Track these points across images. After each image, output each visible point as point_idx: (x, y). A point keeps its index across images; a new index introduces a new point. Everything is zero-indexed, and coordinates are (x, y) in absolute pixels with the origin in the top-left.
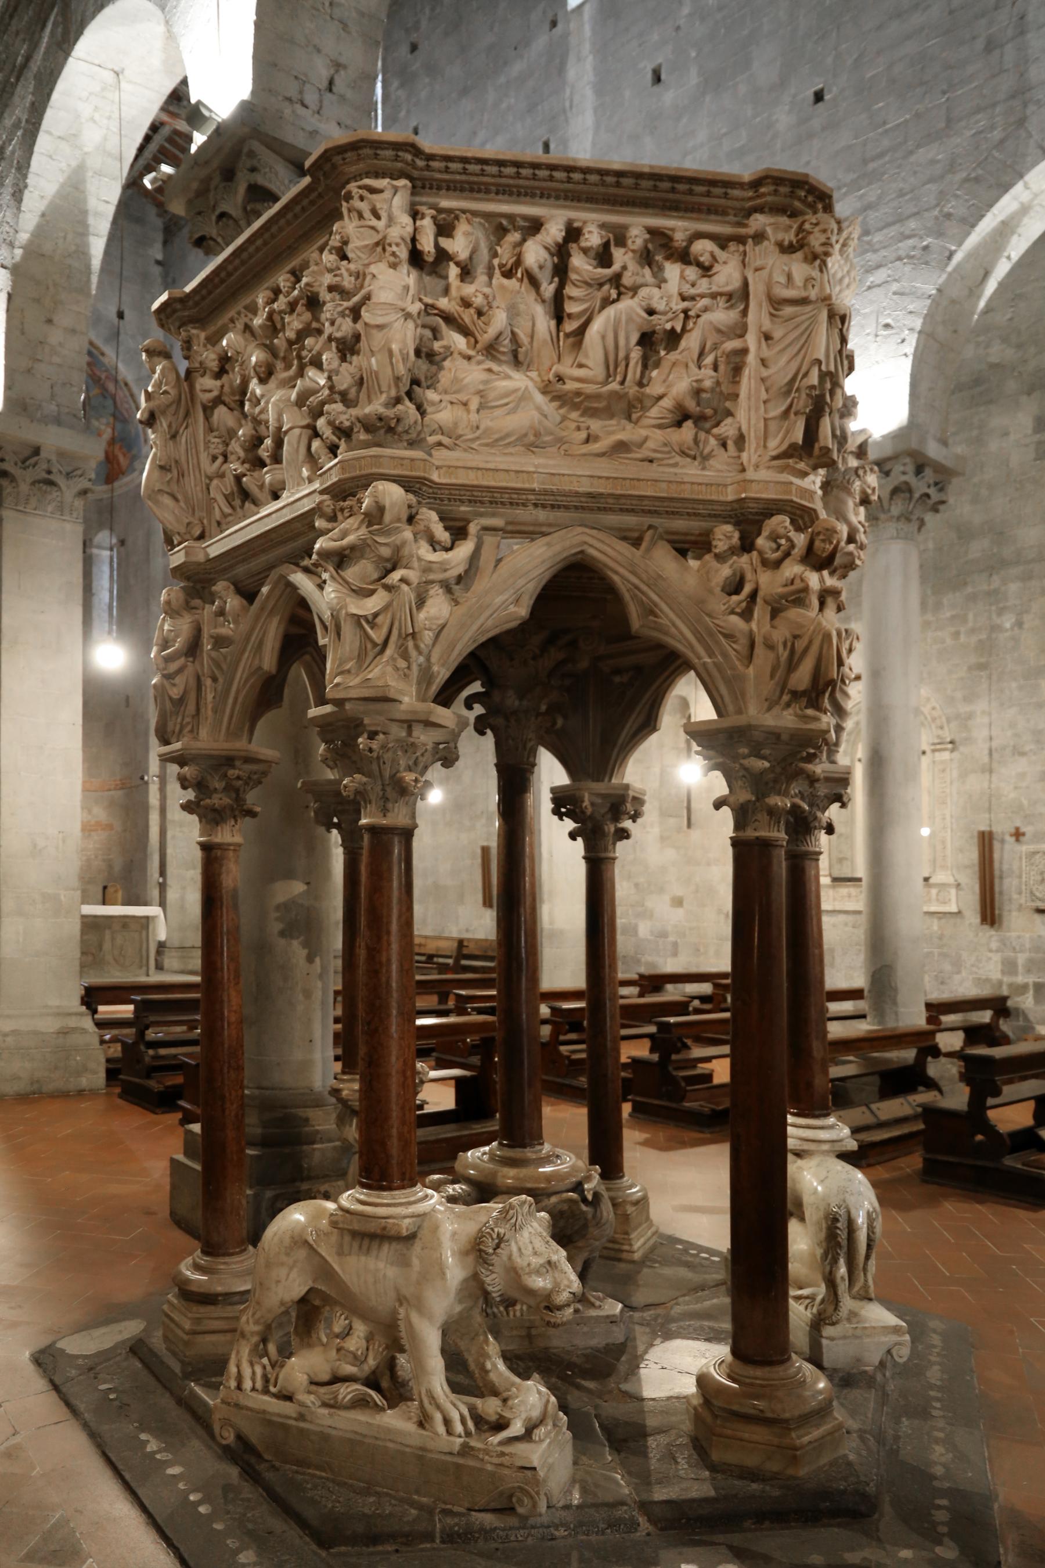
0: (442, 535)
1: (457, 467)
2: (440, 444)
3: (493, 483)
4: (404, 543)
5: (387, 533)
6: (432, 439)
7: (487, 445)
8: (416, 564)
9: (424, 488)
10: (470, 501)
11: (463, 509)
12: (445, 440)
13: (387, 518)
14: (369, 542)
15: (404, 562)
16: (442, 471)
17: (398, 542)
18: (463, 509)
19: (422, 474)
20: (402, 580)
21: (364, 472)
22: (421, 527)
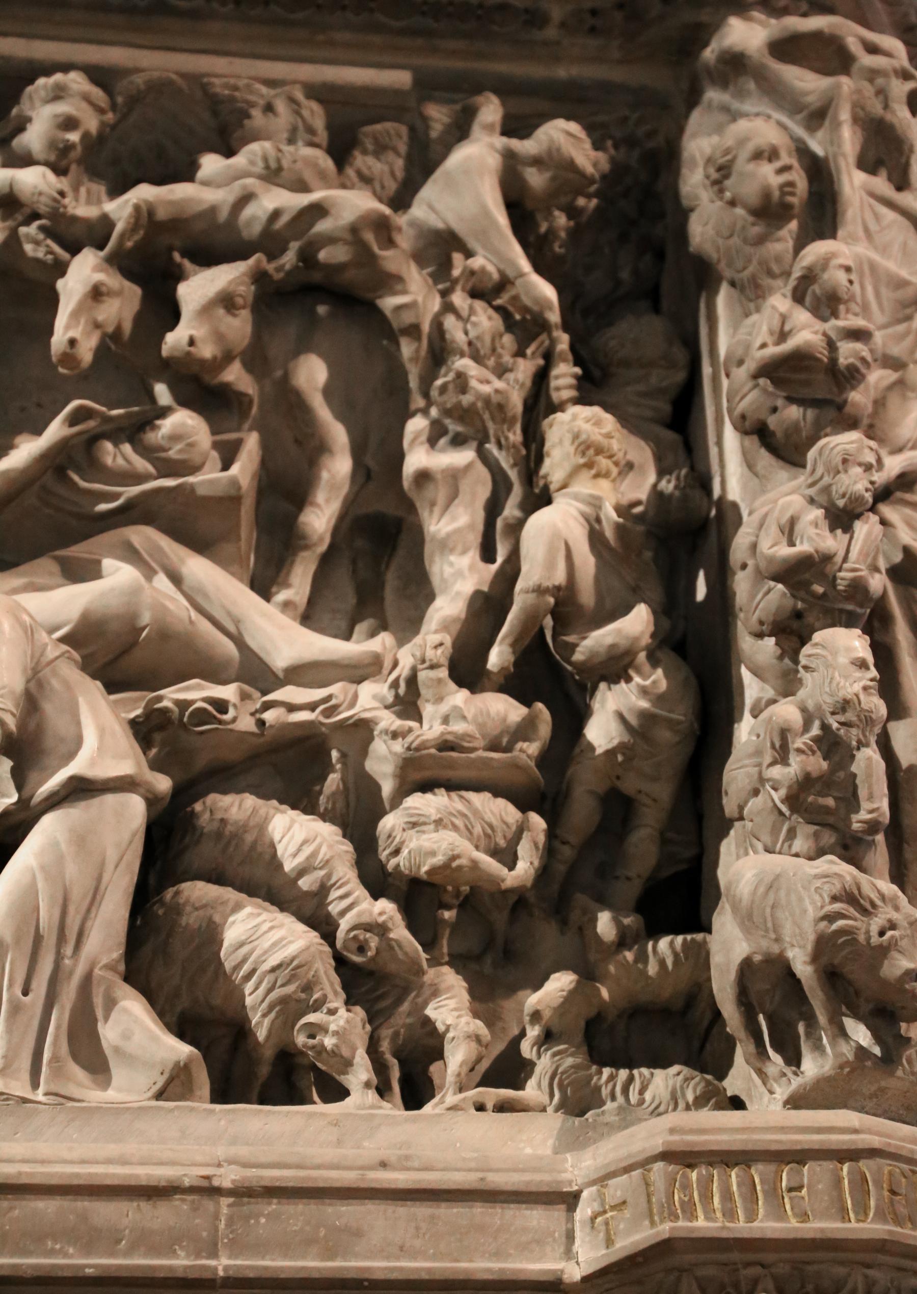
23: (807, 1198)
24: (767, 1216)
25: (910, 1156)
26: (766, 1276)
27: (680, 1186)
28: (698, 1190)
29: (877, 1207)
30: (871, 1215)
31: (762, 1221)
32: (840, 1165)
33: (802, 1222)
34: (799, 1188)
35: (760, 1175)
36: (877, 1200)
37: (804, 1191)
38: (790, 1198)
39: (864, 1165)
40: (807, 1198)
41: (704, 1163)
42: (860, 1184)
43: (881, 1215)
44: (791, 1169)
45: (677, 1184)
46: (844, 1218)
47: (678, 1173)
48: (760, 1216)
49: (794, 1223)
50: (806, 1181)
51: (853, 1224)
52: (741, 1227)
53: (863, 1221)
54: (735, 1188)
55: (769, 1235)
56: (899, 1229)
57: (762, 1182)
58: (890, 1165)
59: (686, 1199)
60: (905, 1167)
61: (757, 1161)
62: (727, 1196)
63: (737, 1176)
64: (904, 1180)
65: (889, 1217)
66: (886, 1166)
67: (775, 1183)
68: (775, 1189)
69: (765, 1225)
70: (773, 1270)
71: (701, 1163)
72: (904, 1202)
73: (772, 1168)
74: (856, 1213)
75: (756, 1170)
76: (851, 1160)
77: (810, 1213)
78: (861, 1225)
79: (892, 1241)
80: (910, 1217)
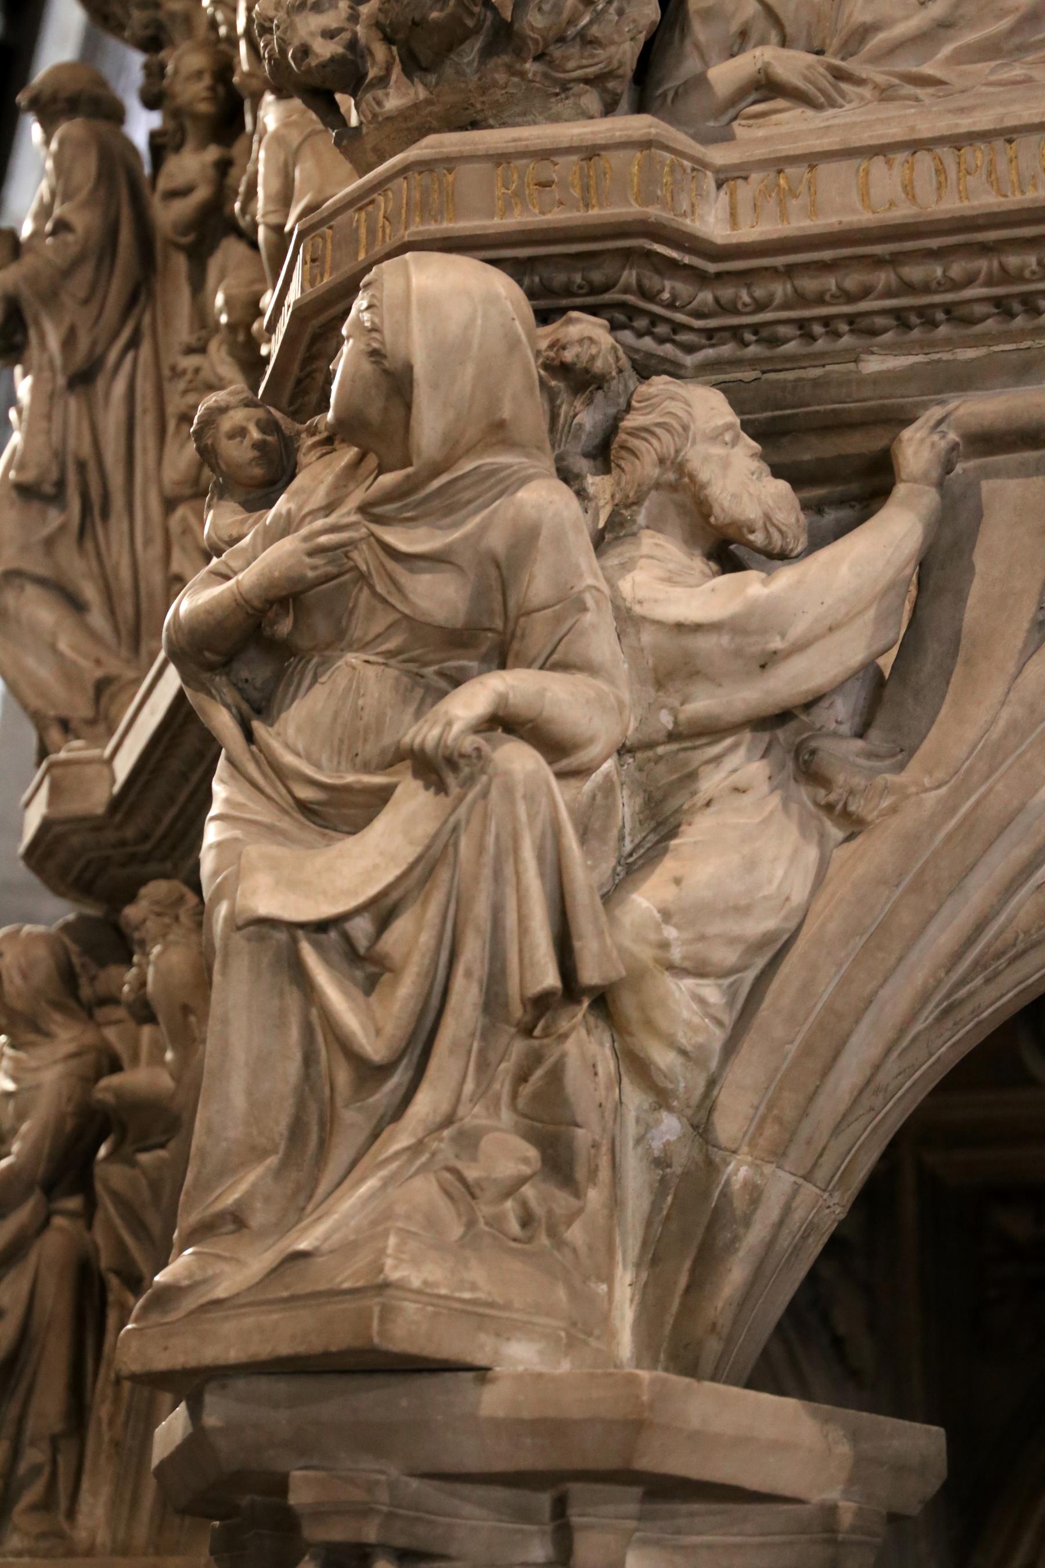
0: (745, 485)
1: (812, 160)
2: (767, 87)
3: (985, 200)
4: (526, 539)
5: (446, 506)
6: (726, 74)
7: (990, 50)
8: (601, 640)
9: (669, 287)
10: (901, 318)
11: (873, 365)
12: (790, 64)
13: (429, 425)
14: (362, 558)
15: (538, 634)
16: (745, 191)
17: (497, 541)
18: (873, 365)
19: (628, 209)
20: (502, 722)
22: (645, 466)
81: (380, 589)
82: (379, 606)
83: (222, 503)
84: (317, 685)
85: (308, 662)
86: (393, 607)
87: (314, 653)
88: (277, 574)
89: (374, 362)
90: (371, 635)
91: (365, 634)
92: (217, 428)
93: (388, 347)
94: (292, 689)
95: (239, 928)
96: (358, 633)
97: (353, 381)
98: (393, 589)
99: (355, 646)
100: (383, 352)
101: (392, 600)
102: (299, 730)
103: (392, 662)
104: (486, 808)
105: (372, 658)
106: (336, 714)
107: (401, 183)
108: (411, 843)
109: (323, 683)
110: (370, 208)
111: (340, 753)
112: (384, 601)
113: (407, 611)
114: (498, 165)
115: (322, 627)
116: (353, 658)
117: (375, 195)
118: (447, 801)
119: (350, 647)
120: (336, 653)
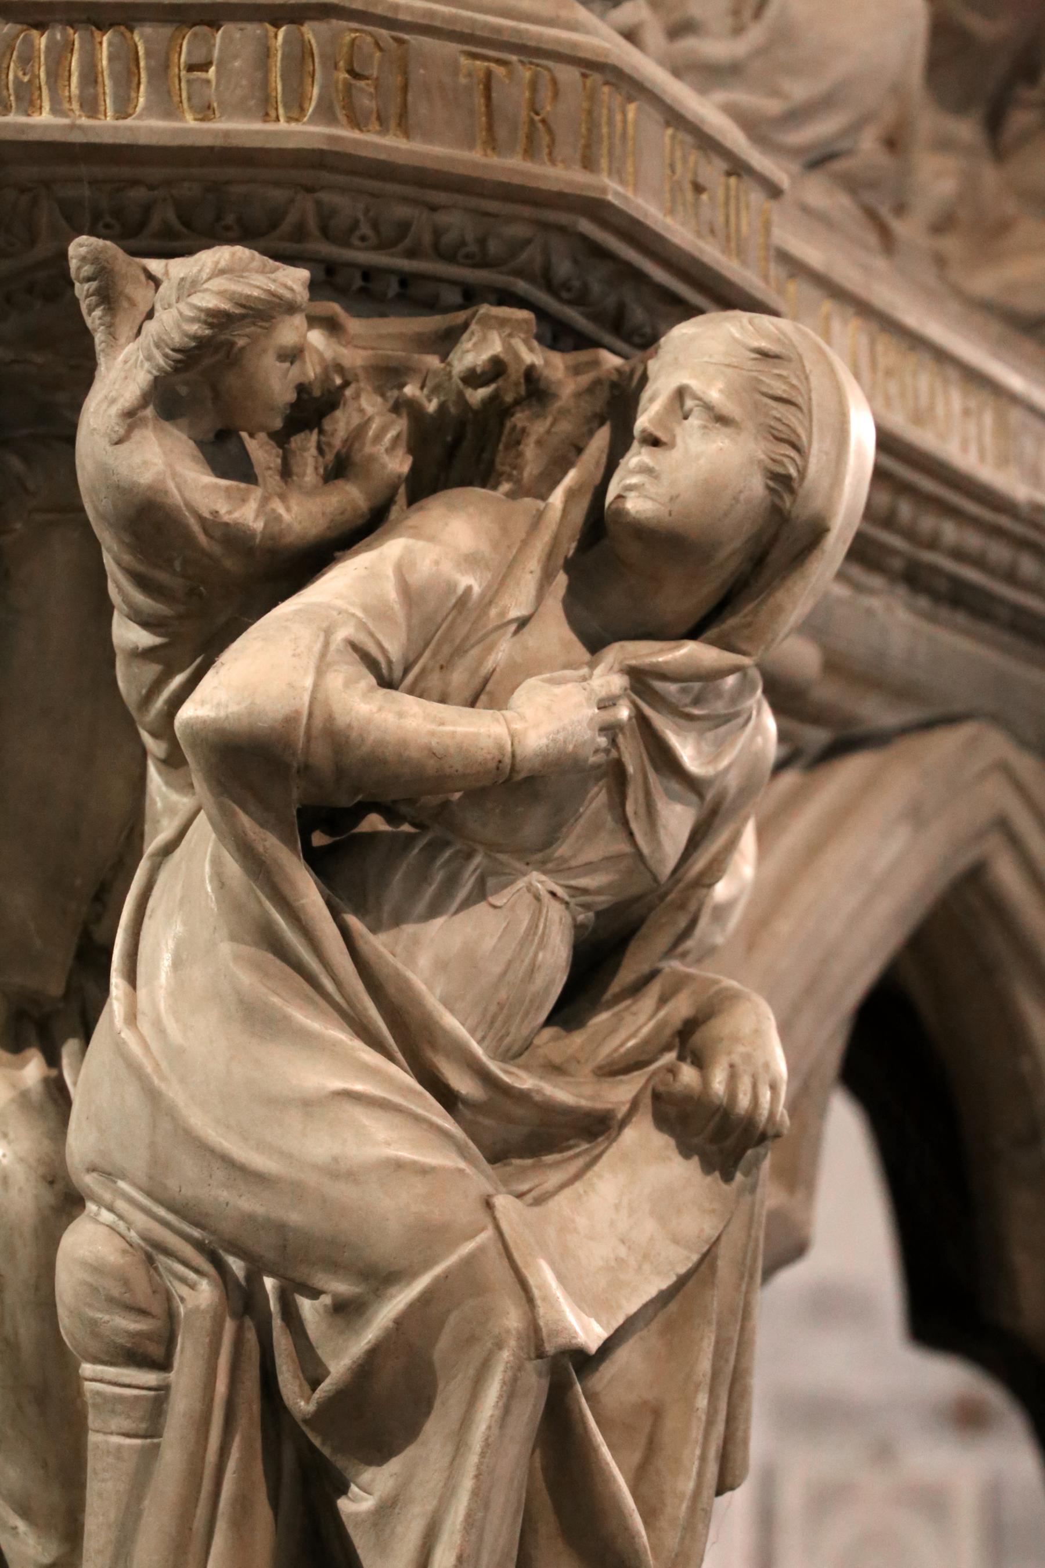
21: (511, 165)
23: (214, 83)
24: (149, 111)
25: (390, 15)
26: (164, 200)
27: (19, 57)
28: (46, 64)
29: (321, 98)
30: (311, 110)
31: (140, 117)
32: (271, 29)
33: (202, 120)
34: (204, 67)
35: (147, 41)
36: (323, 88)
37: (212, 69)
38: (188, 81)
39: (310, 31)
40: (214, 83)
41: (60, 22)
42: (300, 58)
43: (326, 113)
44: (195, 35)
45: (15, 53)
46: (267, 114)
47: (18, 36)
48: (138, 109)
49: (190, 122)
50: (216, 53)
51: (283, 125)
52: (107, 126)
53: (297, 120)
54: (105, 62)
55: (143, 140)
56: (356, 135)
57: (148, 54)
58: (356, 30)
59: (26, 79)
60: (384, 33)
61: (142, 20)
62: (91, 76)
63: (110, 44)
64: (378, 54)
65: (341, 114)
66: (347, 31)
67: (168, 54)
68: (166, 67)
69: (146, 124)
70: (174, 192)
71: (56, 21)
72: (372, 90)
73: (166, 31)
74: (286, 107)
75: (142, 36)
76: (292, 21)
77: (215, 105)
78: (294, 126)
79: (336, 154)
80: (378, 111)
81: (630, 808)
82: (609, 820)
83: (167, 425)
84: (482, 907)
85: (469, 856)
86: (631, 834)
87: (480, 849)
88: (570, 747)
89: (768, 487)
90: (582, 859)
91: (574, 856)
92: (269, 331)
93: (807, 483)
94: (430, 891)
95: (540, 1355)
96: (563, 850)
97: (736, 499)
98: (642, 811)
99: (550, 866)
100: (795, 485)
101: (634, 826)
102: (441, 965)
103: (572, 901)
104: (753, 1205)
105: (560, 891)
106: (509, 964)
107: (568, 74)
108: (676, 1241)
109: (495, 907)
110: (499, 71)
111: (490, 1027)
112: (625, 822)
113: (646, 850)
114: (668, 124)
115: (532, 828)
116: (538, 880)
117: (514, 58)
118: (729, 1189)
119: (542, 867)
120: (519, 865)
